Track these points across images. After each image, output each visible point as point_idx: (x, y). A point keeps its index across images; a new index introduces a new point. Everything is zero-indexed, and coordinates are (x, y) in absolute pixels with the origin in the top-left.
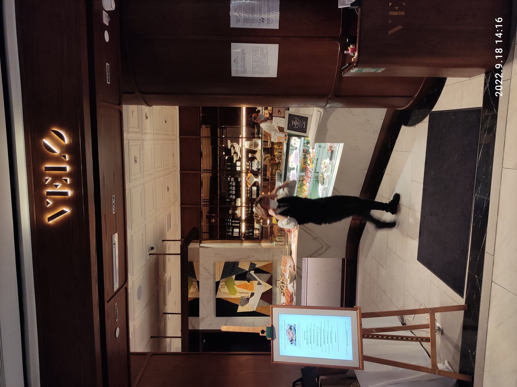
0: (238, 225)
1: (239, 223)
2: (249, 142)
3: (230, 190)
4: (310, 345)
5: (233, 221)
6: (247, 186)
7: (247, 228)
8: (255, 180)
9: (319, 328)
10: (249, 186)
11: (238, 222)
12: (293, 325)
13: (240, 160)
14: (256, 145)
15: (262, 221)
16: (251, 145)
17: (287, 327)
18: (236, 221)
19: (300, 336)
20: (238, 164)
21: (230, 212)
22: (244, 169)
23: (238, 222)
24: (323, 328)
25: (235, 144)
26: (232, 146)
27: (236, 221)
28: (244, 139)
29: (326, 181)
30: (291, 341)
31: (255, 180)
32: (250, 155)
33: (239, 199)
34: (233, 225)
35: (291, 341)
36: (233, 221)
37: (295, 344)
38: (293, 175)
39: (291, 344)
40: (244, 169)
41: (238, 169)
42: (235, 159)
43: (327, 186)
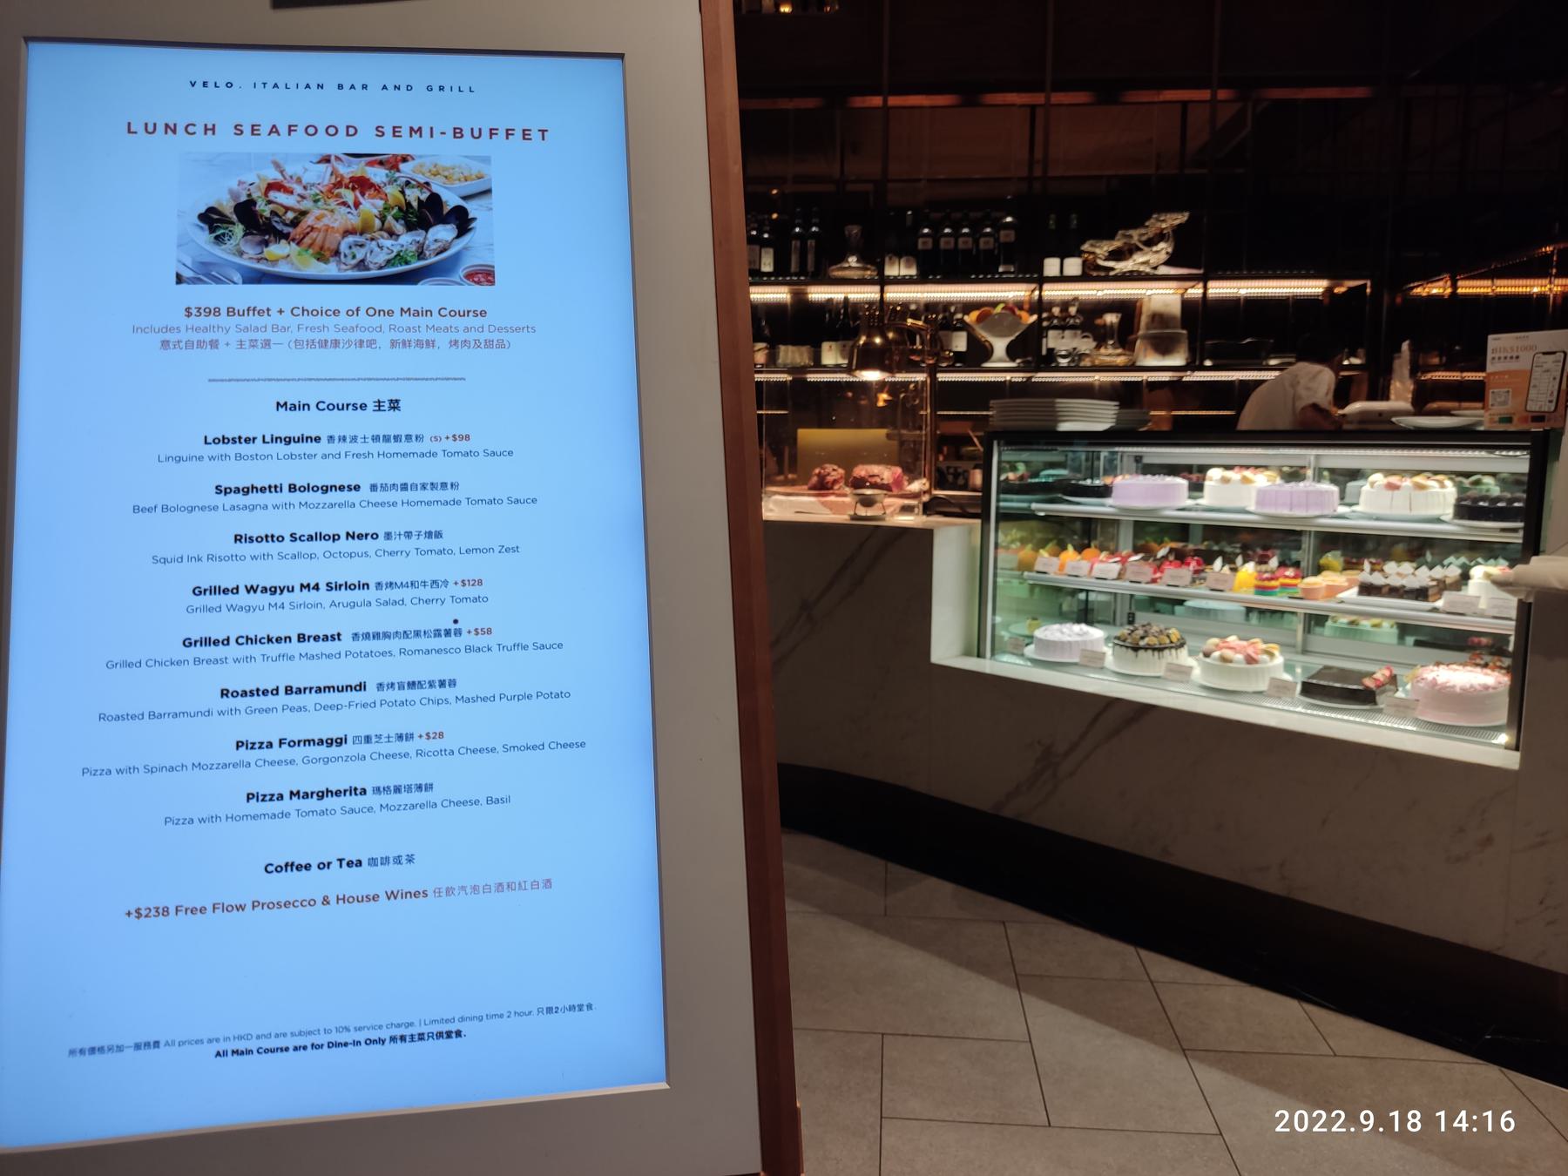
0: (794, 267)
1: (802, 270)
2: (1176, 309)
3: (956, 228)
4: (199, 481)
5: (811, 243)
6: (968, 307)
7: (773, 310)
8: (1000, 345)
9: (470, 617)
10: (971, 318)
11: (810, 267)
12: (478, 247)
13: (1091, 273)
14: (1163, 345)
15: (878, 340)
16: (1159, 319)
17: (439, 161)
18: (811, 259)
19: (320, 339)
20: (1073, 266)
21: (854, 230)
22: (1052, 292)
23: (810, 267)
24: (471, 672)
25: (1164, 248)
26: (1161, 237)
27: (811, 259)
28: (1196, 291)
29: (1151, 665)
30: (246, 210)
31: (1000, 345)
32: (1111, 318)
33: (913, 272)
34: (795, 244)
35: (246, 210)
36: (811, 243)
37: (206, 273)
38: (1135, 492)
39: (211, 219)
40: (1052, 292)
41: (1051, 266)
42: (1102, 249)
43: (1109, 660)
